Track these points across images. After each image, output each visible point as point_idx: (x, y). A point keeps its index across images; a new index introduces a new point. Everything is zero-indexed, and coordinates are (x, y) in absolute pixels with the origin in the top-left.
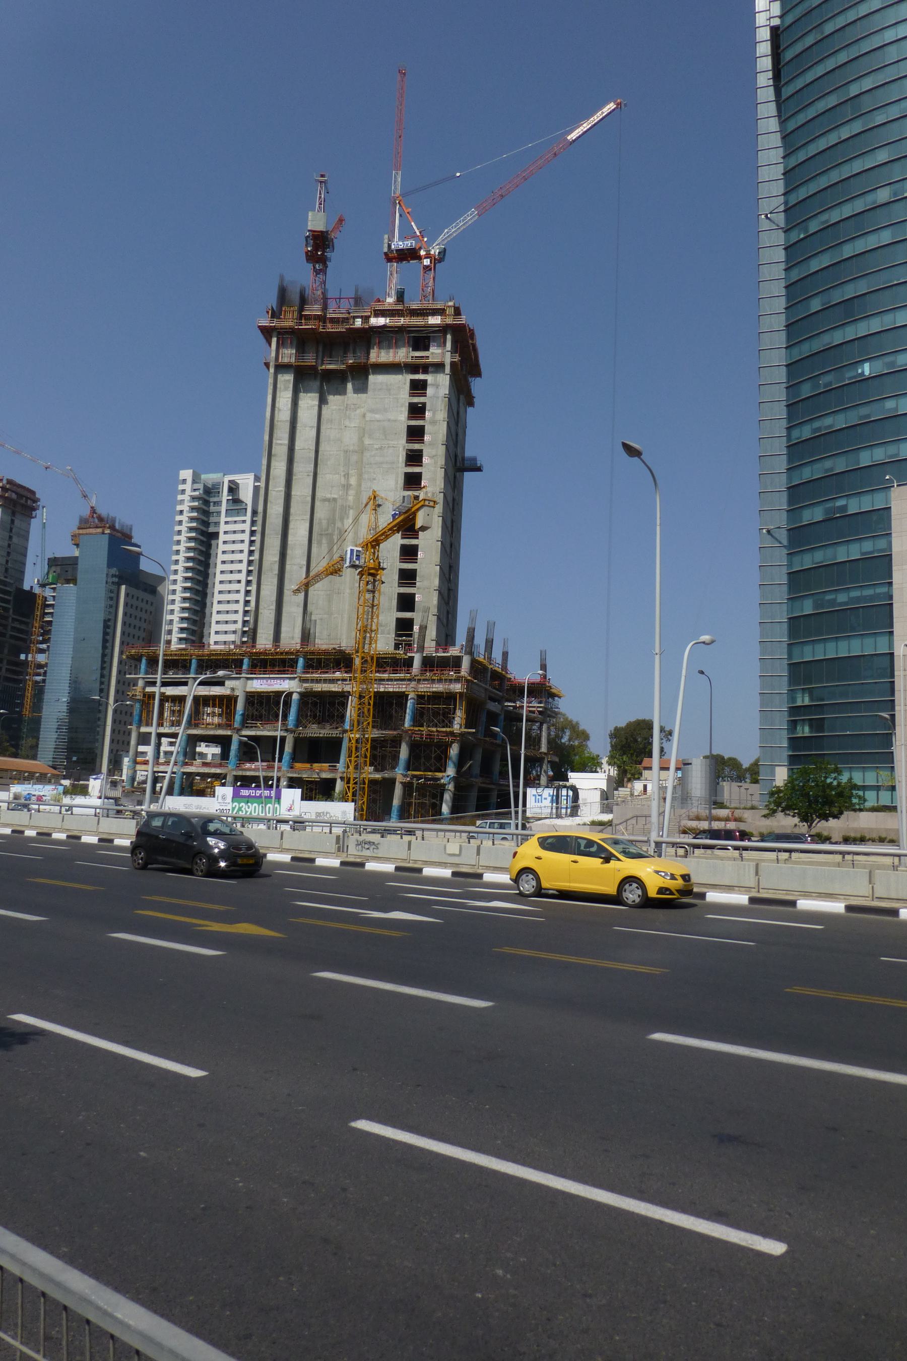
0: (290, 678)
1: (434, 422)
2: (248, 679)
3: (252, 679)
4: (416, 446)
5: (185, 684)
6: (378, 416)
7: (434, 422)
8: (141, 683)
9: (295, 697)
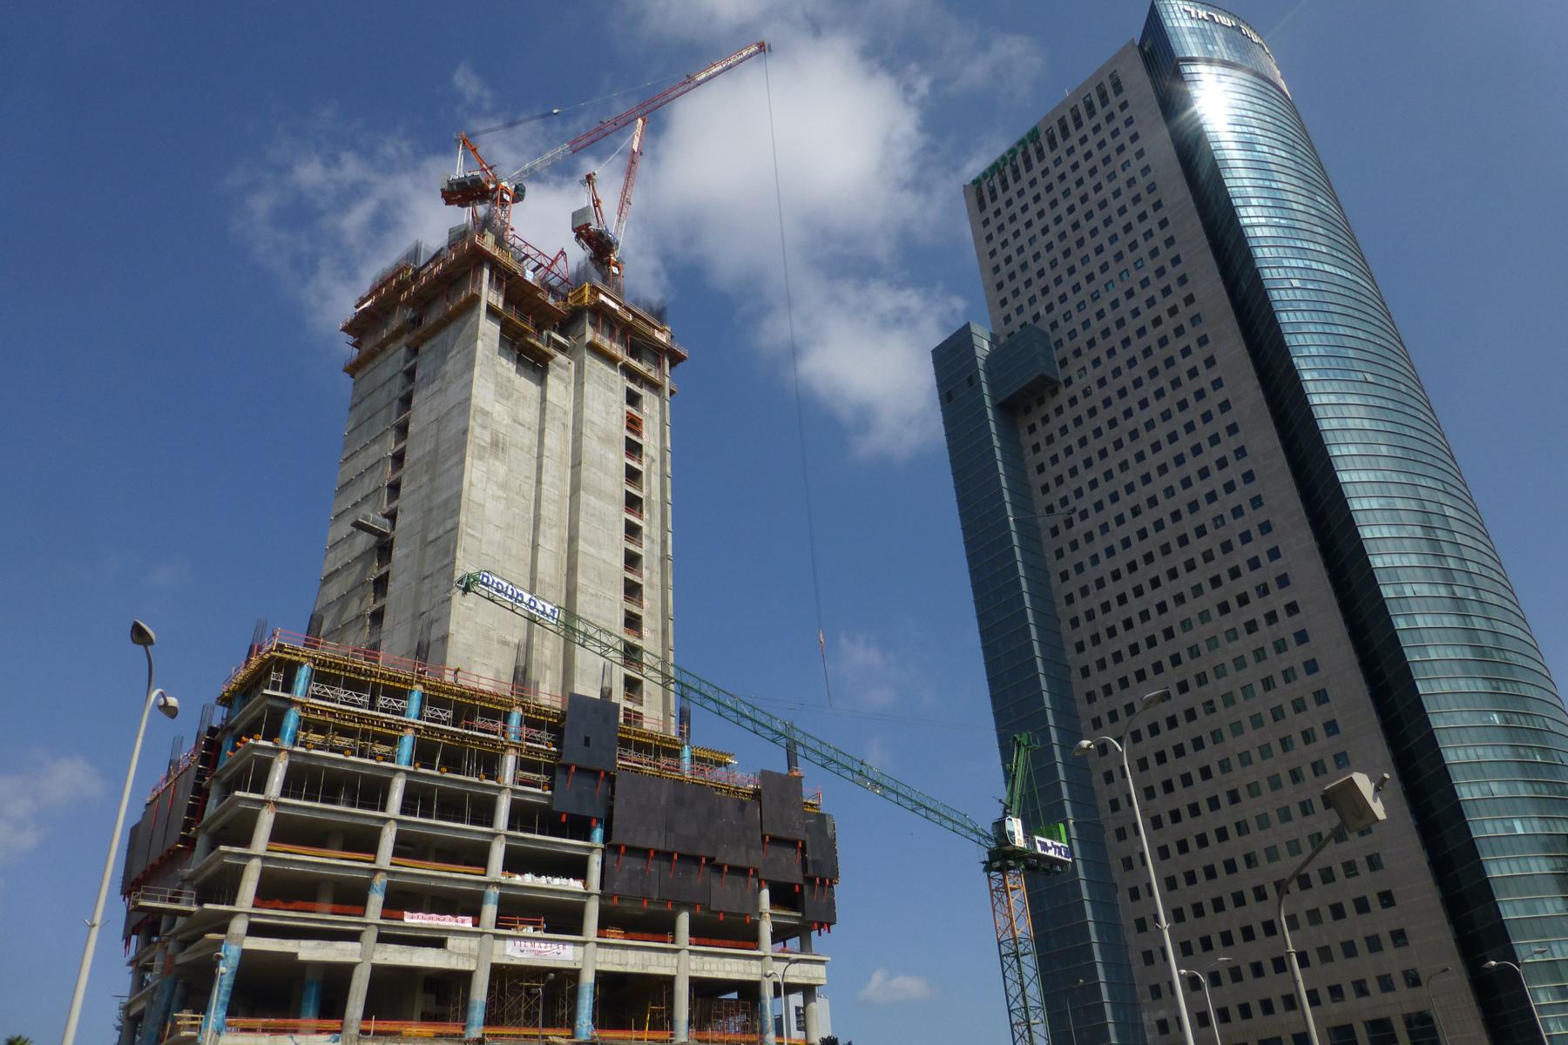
0: (575, 943)
1: (651, 585)
2: (496, 936)
3: (505, 937)
4: (635, 610)
5: (354, 937)
6: (592, 550)
7: (651, 585)
8: (239, 926)
9: (588, 979)
